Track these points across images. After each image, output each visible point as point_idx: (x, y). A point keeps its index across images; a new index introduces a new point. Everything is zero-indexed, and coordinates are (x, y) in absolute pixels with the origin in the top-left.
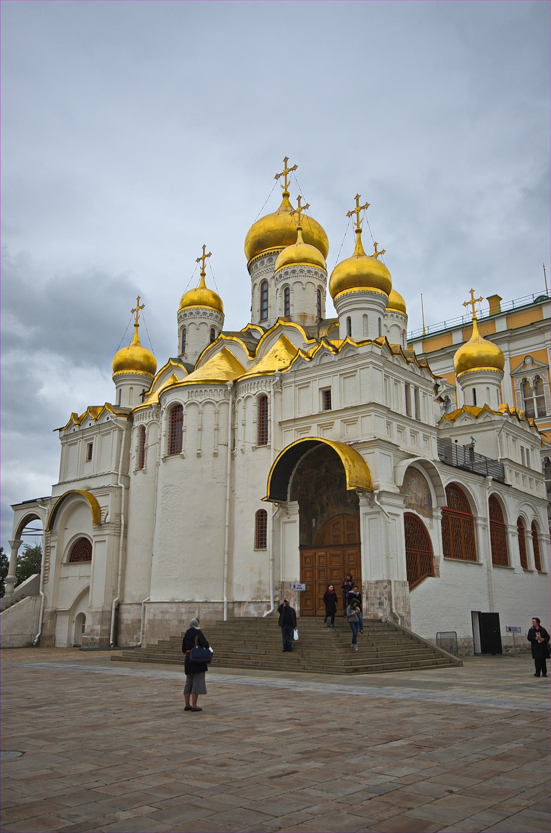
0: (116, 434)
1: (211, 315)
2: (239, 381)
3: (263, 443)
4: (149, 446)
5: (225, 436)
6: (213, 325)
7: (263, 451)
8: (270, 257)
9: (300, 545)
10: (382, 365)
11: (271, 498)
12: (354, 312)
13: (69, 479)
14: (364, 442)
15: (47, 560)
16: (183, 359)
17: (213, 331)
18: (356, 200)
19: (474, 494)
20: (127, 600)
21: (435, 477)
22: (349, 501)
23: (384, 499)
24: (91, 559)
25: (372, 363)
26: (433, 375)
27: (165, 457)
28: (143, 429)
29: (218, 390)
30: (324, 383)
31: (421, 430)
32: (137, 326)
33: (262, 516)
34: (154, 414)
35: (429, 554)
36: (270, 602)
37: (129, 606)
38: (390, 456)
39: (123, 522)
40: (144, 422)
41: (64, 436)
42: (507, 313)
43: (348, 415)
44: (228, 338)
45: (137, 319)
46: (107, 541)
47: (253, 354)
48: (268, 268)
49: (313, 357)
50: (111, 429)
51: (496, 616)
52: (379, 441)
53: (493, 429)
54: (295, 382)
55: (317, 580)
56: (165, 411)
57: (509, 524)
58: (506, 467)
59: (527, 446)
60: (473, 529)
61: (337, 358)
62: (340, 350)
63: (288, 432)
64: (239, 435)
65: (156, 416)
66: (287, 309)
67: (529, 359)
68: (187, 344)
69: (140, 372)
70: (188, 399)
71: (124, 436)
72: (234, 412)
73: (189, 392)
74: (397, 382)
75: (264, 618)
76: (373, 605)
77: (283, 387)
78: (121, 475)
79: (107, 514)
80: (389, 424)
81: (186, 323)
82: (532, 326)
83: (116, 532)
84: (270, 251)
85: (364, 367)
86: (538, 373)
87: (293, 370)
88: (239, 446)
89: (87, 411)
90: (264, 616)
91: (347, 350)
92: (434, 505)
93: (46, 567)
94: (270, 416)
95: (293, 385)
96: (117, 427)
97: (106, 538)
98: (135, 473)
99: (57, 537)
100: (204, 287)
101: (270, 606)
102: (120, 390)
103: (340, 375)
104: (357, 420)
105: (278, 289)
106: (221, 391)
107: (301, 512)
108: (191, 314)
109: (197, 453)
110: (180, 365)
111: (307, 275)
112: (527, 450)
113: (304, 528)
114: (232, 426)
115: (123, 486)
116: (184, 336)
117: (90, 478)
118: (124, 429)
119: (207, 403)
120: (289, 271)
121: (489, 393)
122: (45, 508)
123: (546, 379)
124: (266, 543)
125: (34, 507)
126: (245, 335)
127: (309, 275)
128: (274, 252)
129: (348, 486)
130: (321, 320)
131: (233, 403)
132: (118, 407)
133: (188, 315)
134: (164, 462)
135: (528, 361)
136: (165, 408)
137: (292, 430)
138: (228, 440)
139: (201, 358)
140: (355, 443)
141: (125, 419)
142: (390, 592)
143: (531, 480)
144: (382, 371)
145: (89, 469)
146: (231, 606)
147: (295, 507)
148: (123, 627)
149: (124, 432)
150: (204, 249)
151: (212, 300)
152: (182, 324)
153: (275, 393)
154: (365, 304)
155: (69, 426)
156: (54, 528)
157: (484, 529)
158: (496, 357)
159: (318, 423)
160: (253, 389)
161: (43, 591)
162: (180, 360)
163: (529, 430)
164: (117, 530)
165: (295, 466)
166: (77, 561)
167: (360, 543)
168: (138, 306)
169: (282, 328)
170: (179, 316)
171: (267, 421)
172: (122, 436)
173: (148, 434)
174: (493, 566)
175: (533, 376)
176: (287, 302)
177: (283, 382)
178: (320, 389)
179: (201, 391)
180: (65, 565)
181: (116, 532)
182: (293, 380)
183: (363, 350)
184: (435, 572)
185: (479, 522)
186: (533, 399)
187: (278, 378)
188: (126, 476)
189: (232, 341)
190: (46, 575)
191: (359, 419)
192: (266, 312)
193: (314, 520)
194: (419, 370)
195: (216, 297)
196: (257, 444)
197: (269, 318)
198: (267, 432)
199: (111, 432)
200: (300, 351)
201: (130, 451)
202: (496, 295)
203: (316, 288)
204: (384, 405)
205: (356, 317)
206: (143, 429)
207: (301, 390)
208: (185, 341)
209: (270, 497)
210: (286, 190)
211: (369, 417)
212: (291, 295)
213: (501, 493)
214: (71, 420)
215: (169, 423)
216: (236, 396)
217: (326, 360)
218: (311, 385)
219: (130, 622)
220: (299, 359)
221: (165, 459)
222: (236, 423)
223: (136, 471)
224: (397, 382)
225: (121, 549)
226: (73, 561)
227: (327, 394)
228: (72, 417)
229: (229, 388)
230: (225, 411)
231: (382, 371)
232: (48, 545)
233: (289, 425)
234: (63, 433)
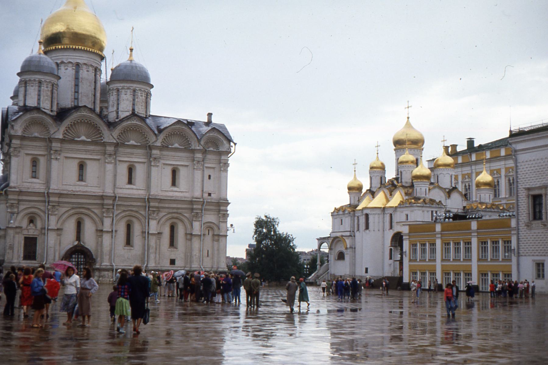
7: (391, 230)
11: (391, 246)
13: (335, 231)
17: (381, 178)
28: (358, 217)
30: (407, 213)
32: (355, 171)
47: (391, 195)
69: (357, 191)
74: (428, 211)
132: (350, 204)
151: (380, 165)
155: (334, 212)
158: (491, 182)
195: (382, 164)
205: (418, 189)
206: (358, 217)
216: (384, 211)
224: (428, 211)
227: (407, 215)
230: (381, 216)
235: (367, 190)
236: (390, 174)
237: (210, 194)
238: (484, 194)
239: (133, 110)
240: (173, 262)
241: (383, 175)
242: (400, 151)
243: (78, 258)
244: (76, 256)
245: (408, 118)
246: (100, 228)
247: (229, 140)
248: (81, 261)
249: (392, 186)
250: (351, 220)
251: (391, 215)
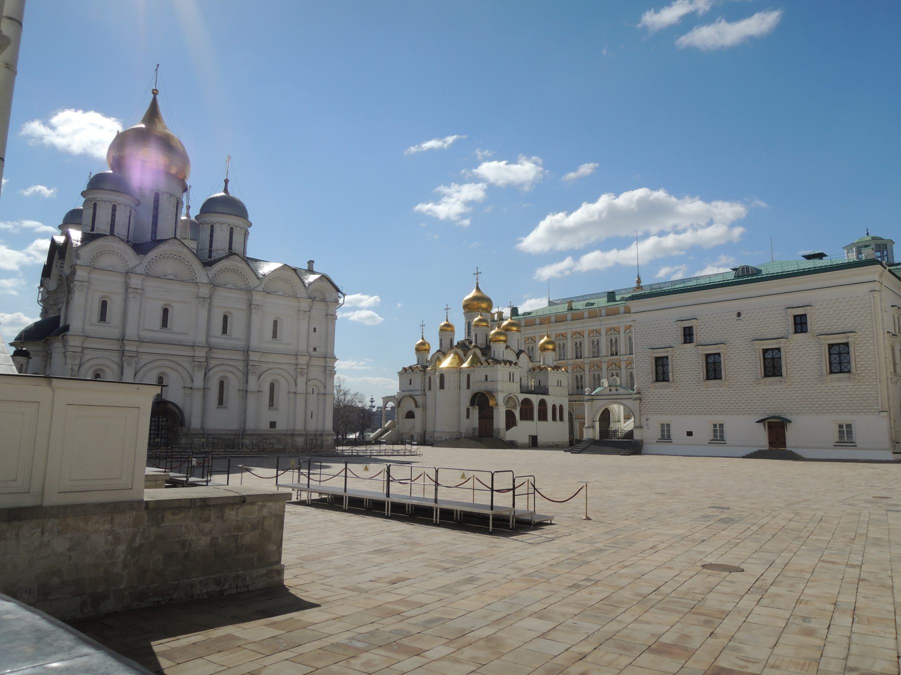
11: (471, 405)
16: (441, 350)
17: (451, 339)
20: (427, 431)
21: (517, 398)
32: (423, 332)
45: (422, 329)
51: (537, 436)
107: (479, 409)
113: (480, 413)
130: (487, 345)
135: (577, 334)
141: (422, 373)
145: (410, 387)
147: (477, 407)
206: (430, 377)
227: (487, 376)
235: (438, 351)
236: (460, 336)
237: (315, 349)
239: (230, 248)
240: (273, 425)
243: (159, 422)
244: (157, 419)
246: (189, 385)
247: (338, 290)
248: (162, 426)
249: (464, 347)
251: (469, 375)
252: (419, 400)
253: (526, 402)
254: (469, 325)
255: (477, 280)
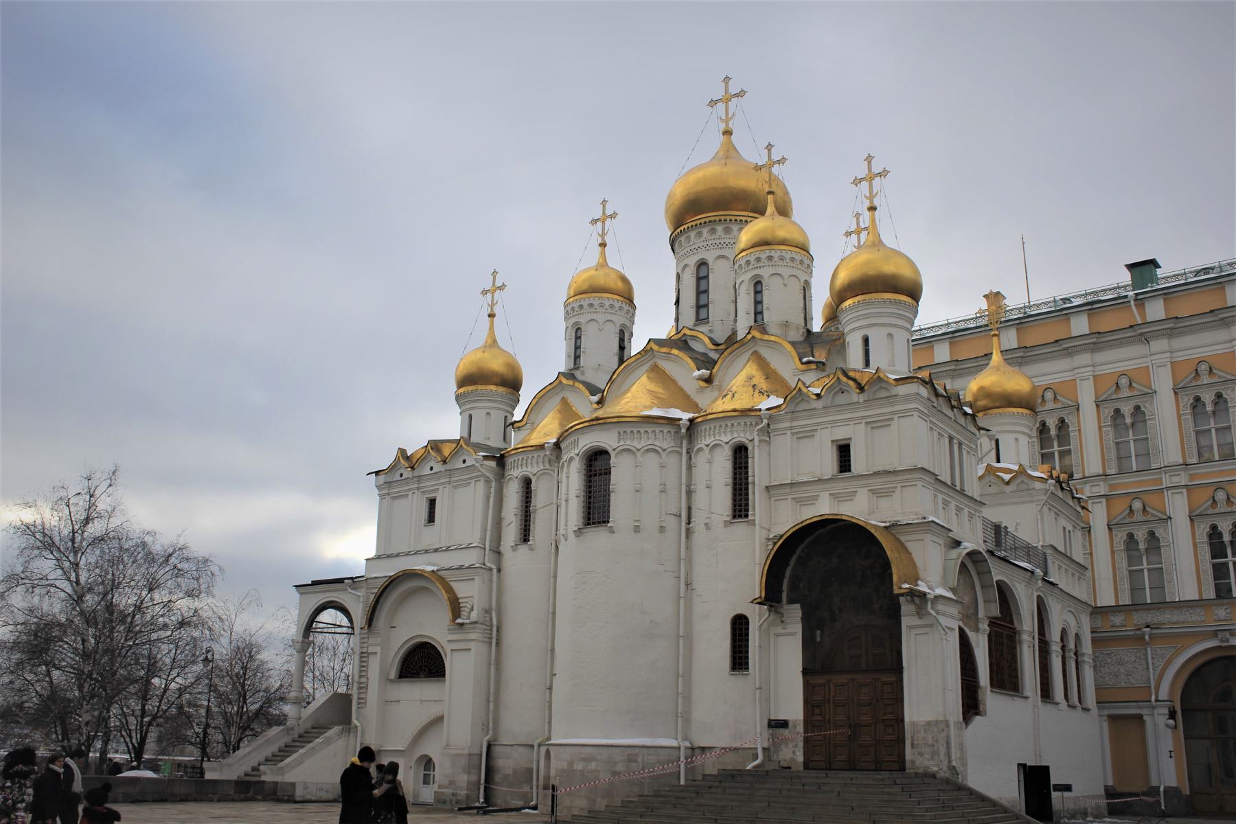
0: (481, 485)
1: (621, 309)
2: (699, 420)
3: (740, 516)
4: (538, 507)
5: (675, 502)
6: (623, 325)
7: (740, 528)
8: (712, 227)
9: (803, 669)
10: (926, 411)
12: (875, 329)
14: (907, 524)
15: (363, 674)
16: (578, 374)
17: (622, 332)
18: (866, 163)
19: (1020, 598)
22: (876, 606)
23: (940, 607)
24: (444, 675)
25: (917, 409)
26: (978, 426)
27: (579, 529)
28: (527, 483)
29: (665, 431)
30: (841, 434)
31: (967, 506)
32: (491, 316)
33: (741, 624)
34: (546, 460)
35: (974, 684)
36: (757, 748)
37: (509, 747)
38: (940, 545)
39: (495, 622)
40: (530, 470)
41: (385, 483)
42: (1018, 322)
43: (878, 483)
44: (664, 350)
45: (492, 305)
46: (473, 650)
48: (709, 243)
49: (822, 394)
50: (472, 478)
52: (932, 524)
53: (1031, 502)
54: (791, 428)
55: (831, 719)
56: (577, 459)
57: (1053, 639)
58: (1049, 558)
59: (1069, 527)
60: (1015, 648)
61: (862, 398)
62: (866, 388)
63: (779, 501)
64: (700, 500)
65: (549, 462)
66: (758, 313)
67: (1049, 393)
68: (584, 352)
69: (501, 389)
70: (618, 442)
71: (493, 490)
72: (690, 468)
73: (619, 432)
75: (748, 770)
76: (921, 754)
77: (771, 435)
78: (490, 550)
79: (472, 609)
80: (935, 496)
81: (583, 319)
82: (1055, 344)
83: (485, 637)
84: (713, 219)
85: (905, 414)
86: (1063, 414)
87: (788, 411)
88: (699, 519)
89: (426, 446)
90: (748, 768)
91: (876, 387)
92: (981, 614)
93: (361, 683)
94: (754, 476)
95: (789, 432)
96: (483, 475)
97: (472, 645)
98: (514, 548)
99: (380, 639)
100: (603, 264)
101: (757, 754)
102: (470, 416)
103: (866, 423)
104: (894, 492)
105: (742, 282)
106: (669, 434)
108: (591, 305)
109: (635, 526)
110: (577, 384)
111: (789, 264)
112: (1069, 531)
113: (808, 643)
114: (687, 486)
115: (493, 566)
116: (578, 338)
117: (436, 550)
118: (493, 479)
119: (648, 450)
120: (764, 256)
121: (1018, 444)
122: (359, 594)
123: (1073, 424)
124: (747, 664)
125: (335, 591)
126: (679, 343)
127: (792, 265)
128: (720, 220)
129: (895, 587)
130: (809, 332)
131: (688, 453)
133: (585, 307)
134: (577, 536)
135: (1049, 395)
136: (578, 455)
137: (787, 499)
138: (681, 508)
139: (614, 377)
140: (893, 524)
141: (493, 464)
142: (948, 737)
143: (1073, 575)
144: (926, 421)
145: (432, 537)
146: (689, 752)
147: (794, 613)
148: (498, 778)
149: (493, 484)
150: (604, 206)
151: (620, 284)
152: (574, 320)
153: (760, 441)
154: (889, 318)
155: (392, 468)
156: (374, 624)
157: (1029, 647)
159: (831, 492)
160: (723, 434)
161: (357, 719)
162: (573, 375)
163: (1071, 503)
164: (486, 633)
165: (794, 552)
166: (414, 677)
167: (902, 668)
168: (494, 284)
169: (756, 343)
170: (569, 308)
171: (747, 484)
172: (490, 490)
173: (536, 490)
174: (1042, 701)
175: (1055, 419)
176: (758, 303)
177: (772, 427)
178: (833, 441)
179: (639, 432)
180: (391, 681)
181: (485, 637)
182: (788, 425)
183: (903, 390)
184: (981, 709)
185: (1025, 637)
186: (1053, 453)
187: (765, 421)
188: (498, 553)
189: (669, 355)
190: (362, 696)
191: (899, 489)
192: (706, 309)
193: (818, 632)
194: (963, 418)
195: (624, 280)
196: (731, 517)
197: (710, 319)
198: (747, 500)
199: (470, 483)
200: (800, 382)
201: (503, 514)
202: (998, 293)
203: (802, 284)
204: (931, 470)
206: (527, 483)
207: (801, 441)
208: (580, 347)
209: (766, 598)
210: (727, 125)
211: (913, 488)
212: (765, 292)
213: (1045, 596)
214: (397, 461)
215: (584, 477)
217: (841, 399)
218: (817, 435)
219: (511, 772)
220: (798, 396)
221: (578, 533)
222: (693, 483)
223: (516, 545)
225: (493, 662)
226: (406, 677)
227: (844, 451)
228: (399, 455)
229: (683, 430)
231: (926, 421)
232: (365, 650)
233: (783, 491)
234: (382, 478)
238: (1012, 437)
241: (628, 323)
242: (713, 231)
245: (728, 133)
250: (488, 498)
252: (471, 592)
253: (1004, 595)
254: (702, 273)
255: (727, 121)
